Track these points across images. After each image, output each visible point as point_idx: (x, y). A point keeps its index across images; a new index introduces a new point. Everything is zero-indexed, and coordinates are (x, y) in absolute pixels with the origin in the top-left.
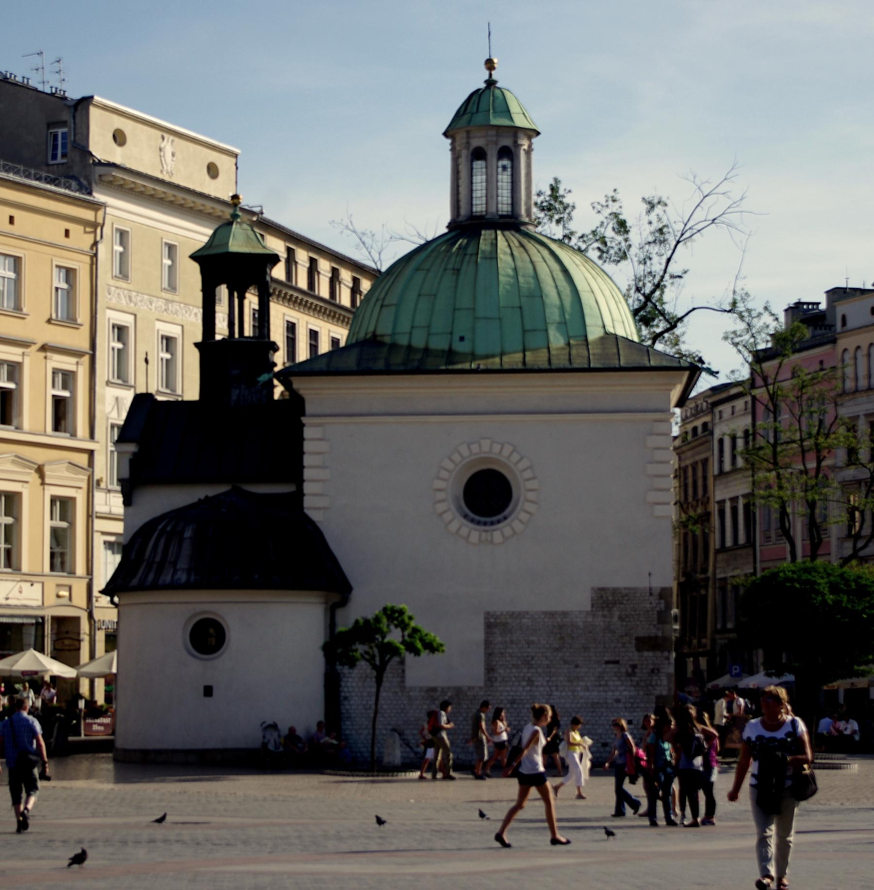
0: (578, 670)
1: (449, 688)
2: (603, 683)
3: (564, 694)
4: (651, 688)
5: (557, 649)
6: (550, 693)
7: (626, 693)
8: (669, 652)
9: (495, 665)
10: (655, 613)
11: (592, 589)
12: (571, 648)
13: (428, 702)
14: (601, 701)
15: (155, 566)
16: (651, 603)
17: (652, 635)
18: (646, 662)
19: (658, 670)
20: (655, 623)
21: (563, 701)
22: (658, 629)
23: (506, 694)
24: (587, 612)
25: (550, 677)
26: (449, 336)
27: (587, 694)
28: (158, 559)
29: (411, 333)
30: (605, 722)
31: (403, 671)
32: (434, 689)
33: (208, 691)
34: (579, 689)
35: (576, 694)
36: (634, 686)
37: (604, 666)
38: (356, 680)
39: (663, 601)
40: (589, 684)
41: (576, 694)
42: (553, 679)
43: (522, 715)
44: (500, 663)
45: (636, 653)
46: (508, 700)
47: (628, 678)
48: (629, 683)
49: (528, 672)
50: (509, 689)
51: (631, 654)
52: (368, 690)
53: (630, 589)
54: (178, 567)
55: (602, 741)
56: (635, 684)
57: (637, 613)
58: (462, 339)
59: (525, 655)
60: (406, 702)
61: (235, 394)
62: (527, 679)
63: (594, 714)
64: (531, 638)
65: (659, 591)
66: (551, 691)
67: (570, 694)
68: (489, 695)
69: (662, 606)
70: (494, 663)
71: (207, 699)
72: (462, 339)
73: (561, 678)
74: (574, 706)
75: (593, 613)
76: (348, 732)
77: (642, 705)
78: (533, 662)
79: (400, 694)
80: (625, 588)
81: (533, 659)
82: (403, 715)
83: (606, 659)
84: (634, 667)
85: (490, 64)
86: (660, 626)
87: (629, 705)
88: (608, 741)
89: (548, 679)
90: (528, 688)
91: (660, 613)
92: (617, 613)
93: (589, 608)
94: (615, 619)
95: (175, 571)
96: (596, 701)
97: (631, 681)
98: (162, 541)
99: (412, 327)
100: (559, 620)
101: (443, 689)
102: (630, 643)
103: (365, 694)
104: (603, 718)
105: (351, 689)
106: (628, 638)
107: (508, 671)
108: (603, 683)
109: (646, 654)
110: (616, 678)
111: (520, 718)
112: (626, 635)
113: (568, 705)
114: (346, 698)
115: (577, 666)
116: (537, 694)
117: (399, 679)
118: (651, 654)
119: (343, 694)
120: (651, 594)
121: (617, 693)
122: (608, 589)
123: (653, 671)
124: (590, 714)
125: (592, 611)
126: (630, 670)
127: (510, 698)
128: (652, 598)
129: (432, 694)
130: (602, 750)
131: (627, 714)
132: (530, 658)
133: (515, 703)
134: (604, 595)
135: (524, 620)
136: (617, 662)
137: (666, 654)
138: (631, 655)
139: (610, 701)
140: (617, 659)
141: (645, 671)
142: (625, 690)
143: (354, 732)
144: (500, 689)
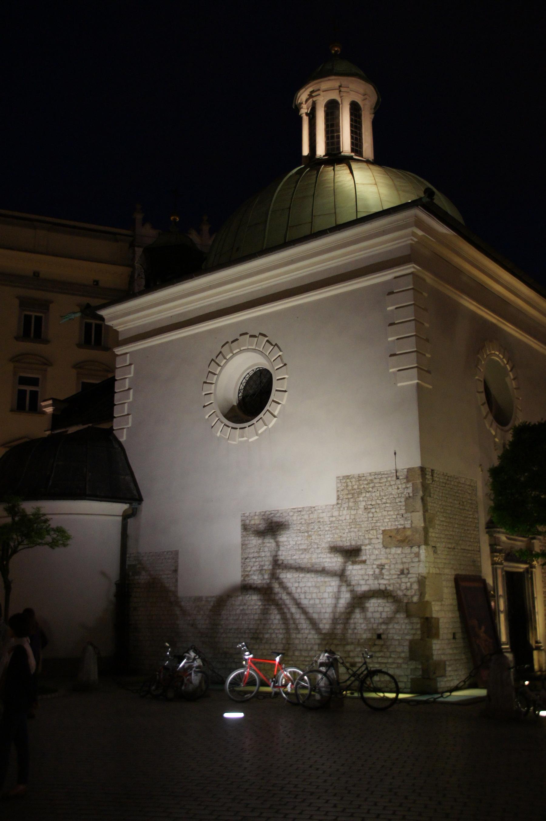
5: (305, 550)
8: (419, 547)
9: (250, 571)
10: (403, 500)
12: (318, 548)
17: (400, 527)
19: (408, 569)
20: (403, 512)
24: (333, 506)
31: (177, 581)
34: (326, 595)
39: (410, 485)
41: (323, 601)
42: (301, 585)
45: (384, 550)
51: (377, 552)
53: (376, 474)
57: (384, 501)
65: (406, 470)
68: (245, 605)
69: (410, 490)
70: (249, 569)
73: (309, 584)
84: (381, 567)
86: (409, 515)
91: (407, 499)
92: (362, 505)
93: (334, 502)
94: (360, 512)
100: (306, 517)
101: (207, 598)
102: (378, 538)
109: (393, 550)
111: (272, 631)
118: (399, 551)
120: (397, 478)
122: (353, 477)
123: (402, 572)
125: (338, 504)
126: (377, 571)
128: (398, 482)
134: (350, 484)
137: (415, 549)
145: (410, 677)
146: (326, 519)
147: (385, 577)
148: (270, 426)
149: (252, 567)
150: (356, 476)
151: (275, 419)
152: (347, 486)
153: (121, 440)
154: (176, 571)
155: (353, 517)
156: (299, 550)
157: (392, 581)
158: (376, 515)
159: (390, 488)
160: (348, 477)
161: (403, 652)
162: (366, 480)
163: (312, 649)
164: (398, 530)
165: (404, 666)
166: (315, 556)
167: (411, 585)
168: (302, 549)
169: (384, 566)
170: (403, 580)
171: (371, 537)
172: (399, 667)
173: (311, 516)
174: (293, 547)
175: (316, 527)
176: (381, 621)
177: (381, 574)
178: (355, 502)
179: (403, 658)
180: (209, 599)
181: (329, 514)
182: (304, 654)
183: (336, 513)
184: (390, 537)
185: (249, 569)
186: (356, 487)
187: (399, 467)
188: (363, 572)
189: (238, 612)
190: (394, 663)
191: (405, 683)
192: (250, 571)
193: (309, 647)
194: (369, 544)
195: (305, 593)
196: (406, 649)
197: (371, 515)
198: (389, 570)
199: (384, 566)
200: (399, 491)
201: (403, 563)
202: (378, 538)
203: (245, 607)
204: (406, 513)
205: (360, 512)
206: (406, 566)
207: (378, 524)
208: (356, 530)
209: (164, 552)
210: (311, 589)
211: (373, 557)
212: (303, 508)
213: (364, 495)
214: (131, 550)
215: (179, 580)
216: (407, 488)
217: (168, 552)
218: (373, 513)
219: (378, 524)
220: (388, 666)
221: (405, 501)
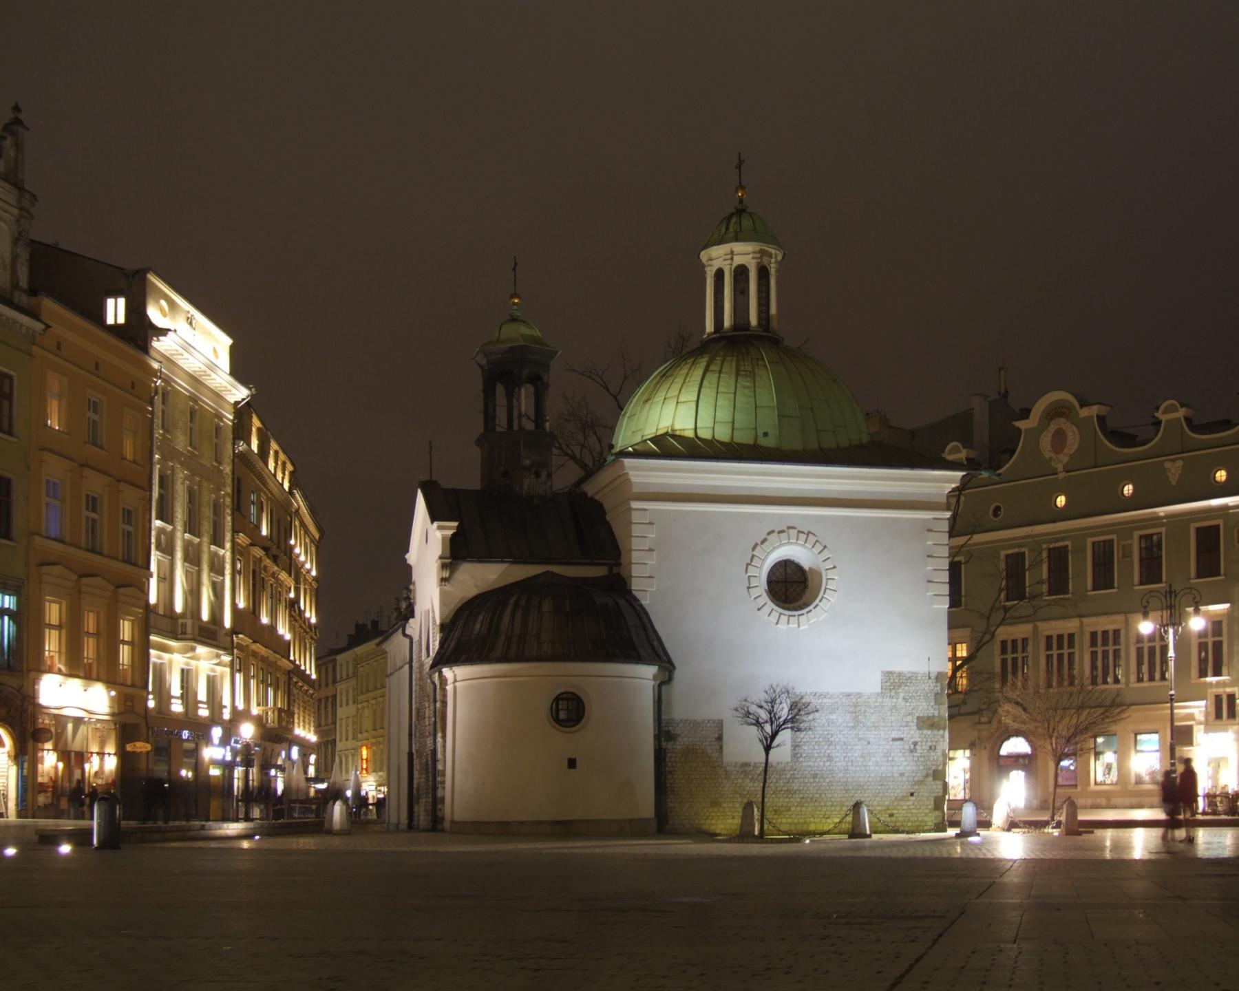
0: (868, 746)
2: (890, 758)
5: (853, 727)
6: (846, 768)
7: (908, 768)
8: (944, 730)
9: (800, 742)
10: (933, 695)
11: (882, 672)
13: (742, 776)
17: (930, 715)
18: (925, 740)
20: (932, 704)
22: (935, 710)
24: (878, 694)
25: (847, 753)
27: (877, 768)
31: (721, 747)
32: (747, 765)
33: (572, 763)
34: (870, 763)
35: (868, 768)
36: (916, 761)
37: (891, 743)
39: (939, 684)
40: (879, 759)
42: (849, 755)
43: (823, 788)
44: (805, 740)
45: (918, 731)
46: (811, 774)
47: (911, 754)
48: (911, 758)
49: (828, 749)
51: (912, 732)
53: (913, 673)
55: (889, 812)
56: (916, 759)
57: (918, 694)
59: (826, 733)
62: (827, 755)
63: (883, 787)
64: (831, 717)
65: (936, 674)
66: (847, 766)
67: (863, 768)
68: (795, 770)
69: (939, 688)
70: (799, 740)
71: (572, 770)
73: (856, 755)
75: (882, 694)
76: (672, 805)
78: (832, 739)
80: (909, 672)
81: (832, 735)
83: (893, 736)
84: (915, 744)
86: (937, 707)
88: (895, 812)
89: (845, 755)
90: (829, 763)
91: (936, 694)
92: (902, 695)
93: (880, 691)
94: (900, 700)
96: (884, 775)
97: (913, 756)
98: (519, 615)
101: (755, 763)
102: (913, 722)
105: (674, 764)
106: (911, 717)
108: (890, 758)
109: (925, 732)
110: (901, 754)
112: (909, 714)
113: (861, 779)
114: (670, 772)
116: (835, 768)
118: (929, 732)
119: (667, 769)
120: (930, 678)
121: (901, 768)
122: (895, 673)
123: (931, 748)
124: (879, 787)
125: (882, 693)
126: (912, 747)
127: (813, 772)
128: (930, 681)
130: (889, 819)
132: (830, 736)
133: (816, 777)
135: (825, 700)
136: (902, 739)
137: (941, 732)
138: (913, 734)
139: (896, 775)
140: (902, 736)
142: (908, 765)
145: (934, 822)
146: (872, 704)
147: (918, 751)
148: (821, 619)
149: (802, 739)
150: (897, 672)
151: (826, 614)
152: (890, 679)
153: (643, 602)
154: (720, 738)
155: (893, 704)
156: (847, 727)
157: (923, 755)
158: (912, 704)
159: (923, 685)
160: (891, 672)
161: (930, 805)
162: (903, 677)
164: (929, 717)
165: (930, 815)
166: (861, 732)
167: (938, 758)
168: (849, 727)
169: (917, 743)
170: (932, 754)
171: (907, 720)
172: (927, 815)
173: (859, 700)
174: (841, 724)
175: (863, 709)
176: (913, 783)
177: (915, 748)
178: (896, 693)
179: (930, 809)
180: (758, 765)
181: (874, 700)
183: (880, 700)
184: (923, 722)
186: (896, 681)
187: (932, 670)
188: (901, 747)
189: (788, 776)
190: (922, 813)
192: (800, 742)
194: (907, 726)
195: (852, 761)
196: (932, 803)
197: (908, 704)
198: (922, 746)
199: (917, 743)
201: (932, 741)
202: (913, 722)
203: (796, 772)
204: (936, 702)
205: (900, 700)
206: (934, 743)
207: (914, 711)
208: (896, 714)
209: (703, 721)
210: (858, 758)
211: (910, 736)
212: (852, 693)
213: (903, 687)
214: (664, 717)
215: (725, 748)
216: (937, 686)
217: (709, 721)
218: (910, 703)
219: (914, 711)
220: (918, 815)
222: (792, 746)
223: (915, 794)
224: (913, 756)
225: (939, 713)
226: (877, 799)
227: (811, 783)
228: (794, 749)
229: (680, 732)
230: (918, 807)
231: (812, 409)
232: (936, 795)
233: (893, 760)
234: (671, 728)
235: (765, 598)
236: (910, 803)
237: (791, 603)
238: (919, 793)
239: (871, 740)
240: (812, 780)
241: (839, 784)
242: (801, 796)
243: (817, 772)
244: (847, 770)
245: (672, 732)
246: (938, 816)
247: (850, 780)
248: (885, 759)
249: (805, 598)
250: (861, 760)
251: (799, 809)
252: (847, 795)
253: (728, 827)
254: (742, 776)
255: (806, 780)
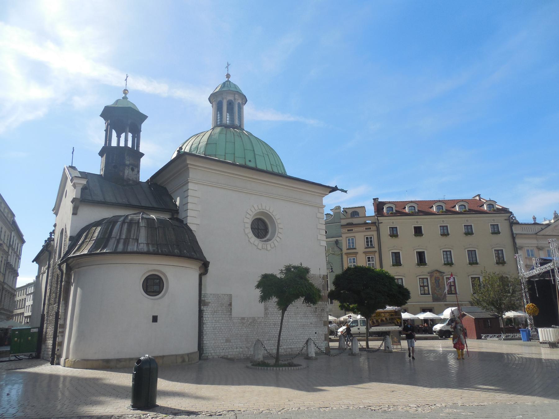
0: (297, 309)
1: (250, 318)
3: (293, 320)
4: (321, 317)
6: (288, 320)
9: (268, 307)
10: (322, 285)
13: (241, 325)
14: (306, 324)
15: (122, 241)
16: (320, 281)
19: (324, 310)
21: (293, 324)
23: (272, 320)
26: (244, 159)
27: (301, 320)
28: (124, 236)
29: (225, 155)
30: (308, 333)
31: (231, 309)
32: (243, 319)
33: (155, 319)
36: (317, 317)
37: (306, 308)
38: (210, 314)
47: (315, 313)
50: (273, 318)
52: (215, 319)
54: (139, 242)
58: (250, 161)
60: (232, 325)
61: (126, 172)
66: (289, 319)
67: (295, 320)
68: (266, 321)
70: (268, 306)
72: (250, 161)
73: (292, 313)
74: (297, 326)
77: (319, 325)
79: (229, 321)
82: (230, 332)
85: (228, 76)
87: (315, 325)
95: (138, 244)
96: (304, 323)
97: (315, 314)
98: (125, 226)
99: (226, 153)
101: (247, 318)
103: (214, 321)
104: (307, 332)
105: (207, 319)
107: (273, 309)
115: (297, 308)
117: (229, 313)
121: (311, 320)
124: (302, 330)
127: (274, 323)
129: (243, 321)
131: (314, 330)
137: (326, 303)
139: (309, 324)
141: (320, 310)
143: (208, 342)
144: (270, 318)
154: (230, 305)
161: (323, 338)
163: (293, 339)
165: (323, 343)
177: (316, 310)
182: (291, 341)
185: (268, 306)
191: (324, 349)
193: (293, 338)
196: (324, 337)
200: (320, 282)
206: (323, 309)
214: (203, 292)
221: (323, 286)
222: (265, 309)
223: (317, 333)
224: (315, 314)
225: (324, 294)
226: (302, 336)
227: (273, 328)
228: (265, 311)
229: (210, 301)
230: (318, 339)
231: (268, 155)
232: (325, 333)
233: (308, 316)
234: (205, 299)
235: (251, 235)
236: (315, 337)
237: (261, 238)
238: (318, 332)
239: (298, 306)
240: (273, 326)
241: (286, 328)
242: (269, 335)
243: (276, 322)
244: (289, 321)
245: (206, 301)
246: (326, 344)
247: (290, 326)
248: (304, 315)
249: (268, 237)
250: (295, 316)
251: (268, 342)
252: (289, 334)
253: (234, 353)
254: (241, 325)
255: (271, 326)
